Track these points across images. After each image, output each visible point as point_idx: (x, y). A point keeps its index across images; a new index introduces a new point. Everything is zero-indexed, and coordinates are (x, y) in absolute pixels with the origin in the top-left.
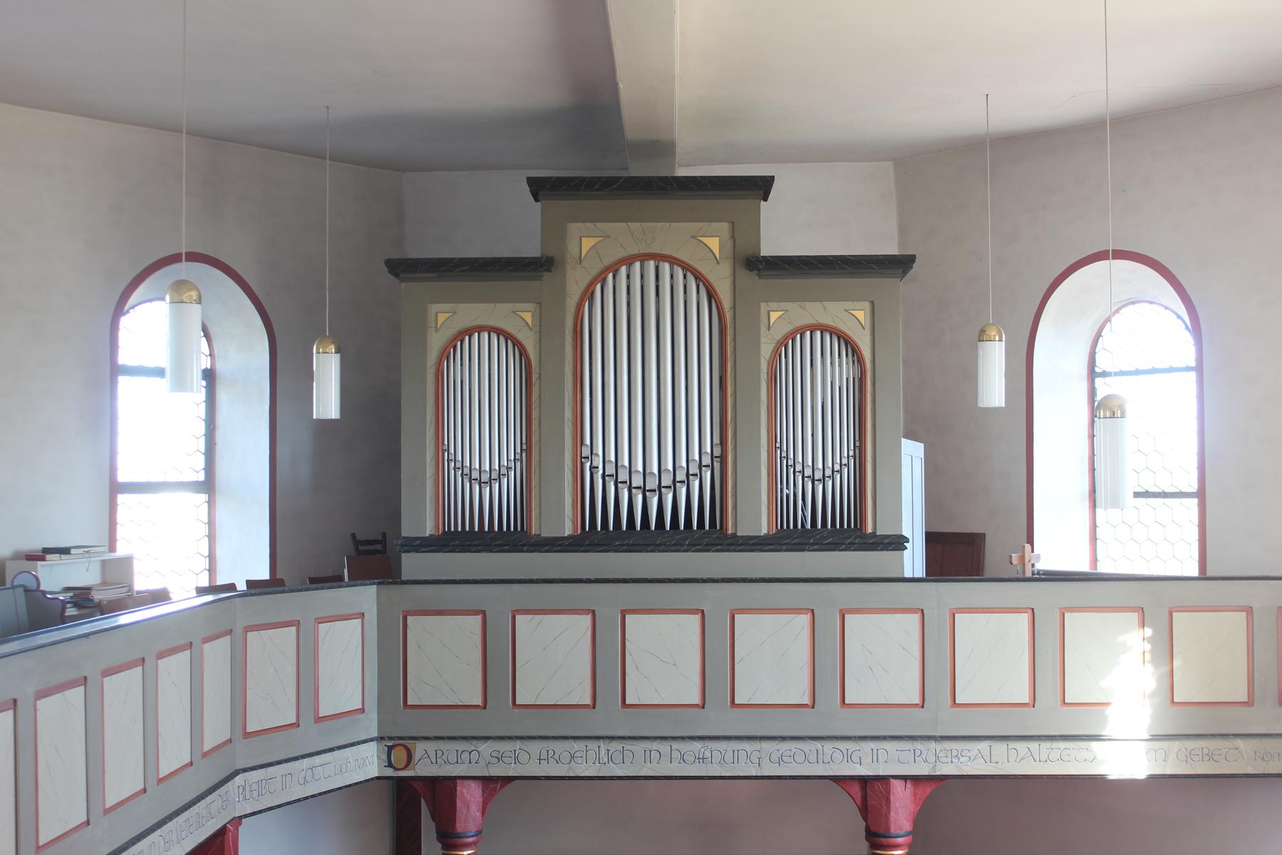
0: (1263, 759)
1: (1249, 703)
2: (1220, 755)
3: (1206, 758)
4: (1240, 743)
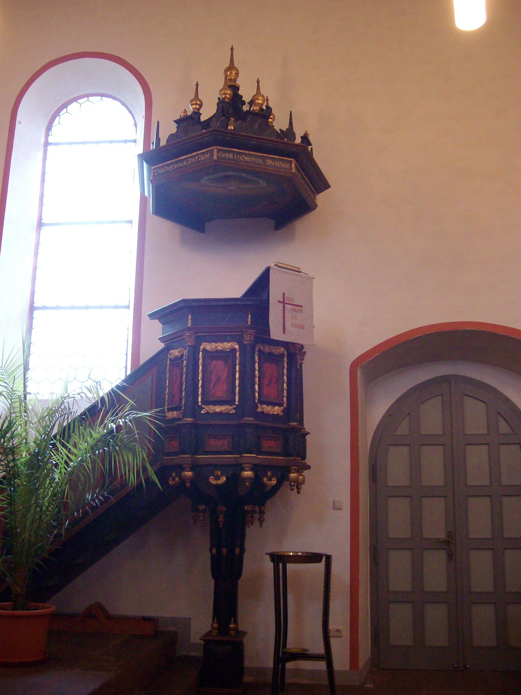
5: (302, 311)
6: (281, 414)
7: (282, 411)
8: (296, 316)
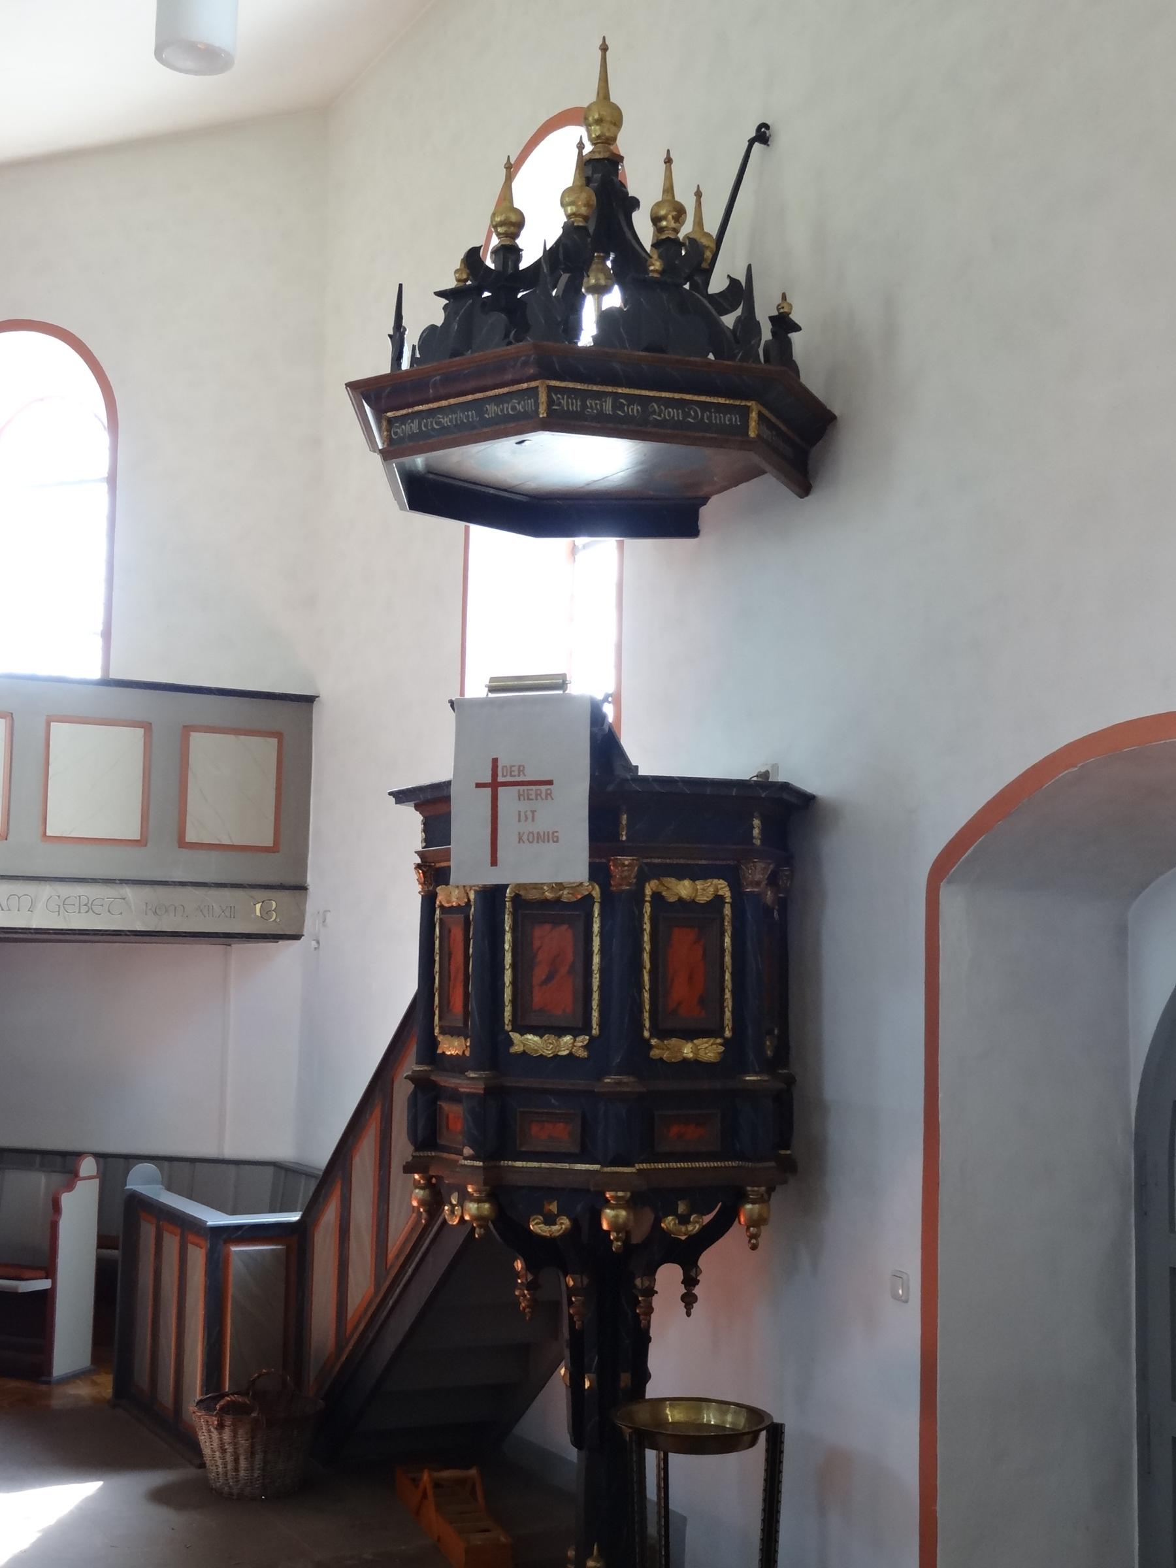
0: (155, 913)
1: (140, 843)
2: (102, 905)
3: (84, 909)
4: (128, 891)
5: (549, 794)
6: (583, 1054)
7: (585, 1047)
8: (533, 812)
